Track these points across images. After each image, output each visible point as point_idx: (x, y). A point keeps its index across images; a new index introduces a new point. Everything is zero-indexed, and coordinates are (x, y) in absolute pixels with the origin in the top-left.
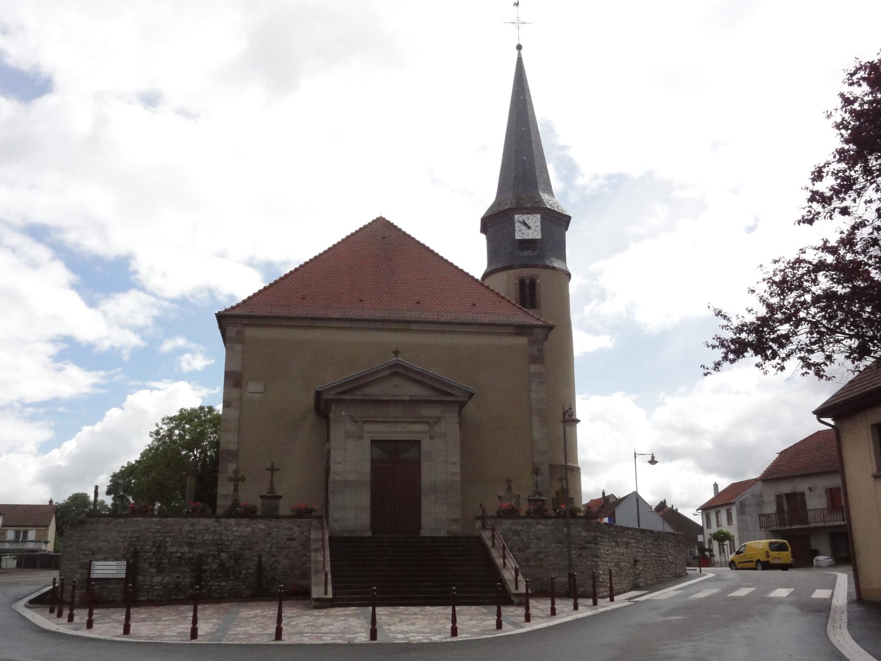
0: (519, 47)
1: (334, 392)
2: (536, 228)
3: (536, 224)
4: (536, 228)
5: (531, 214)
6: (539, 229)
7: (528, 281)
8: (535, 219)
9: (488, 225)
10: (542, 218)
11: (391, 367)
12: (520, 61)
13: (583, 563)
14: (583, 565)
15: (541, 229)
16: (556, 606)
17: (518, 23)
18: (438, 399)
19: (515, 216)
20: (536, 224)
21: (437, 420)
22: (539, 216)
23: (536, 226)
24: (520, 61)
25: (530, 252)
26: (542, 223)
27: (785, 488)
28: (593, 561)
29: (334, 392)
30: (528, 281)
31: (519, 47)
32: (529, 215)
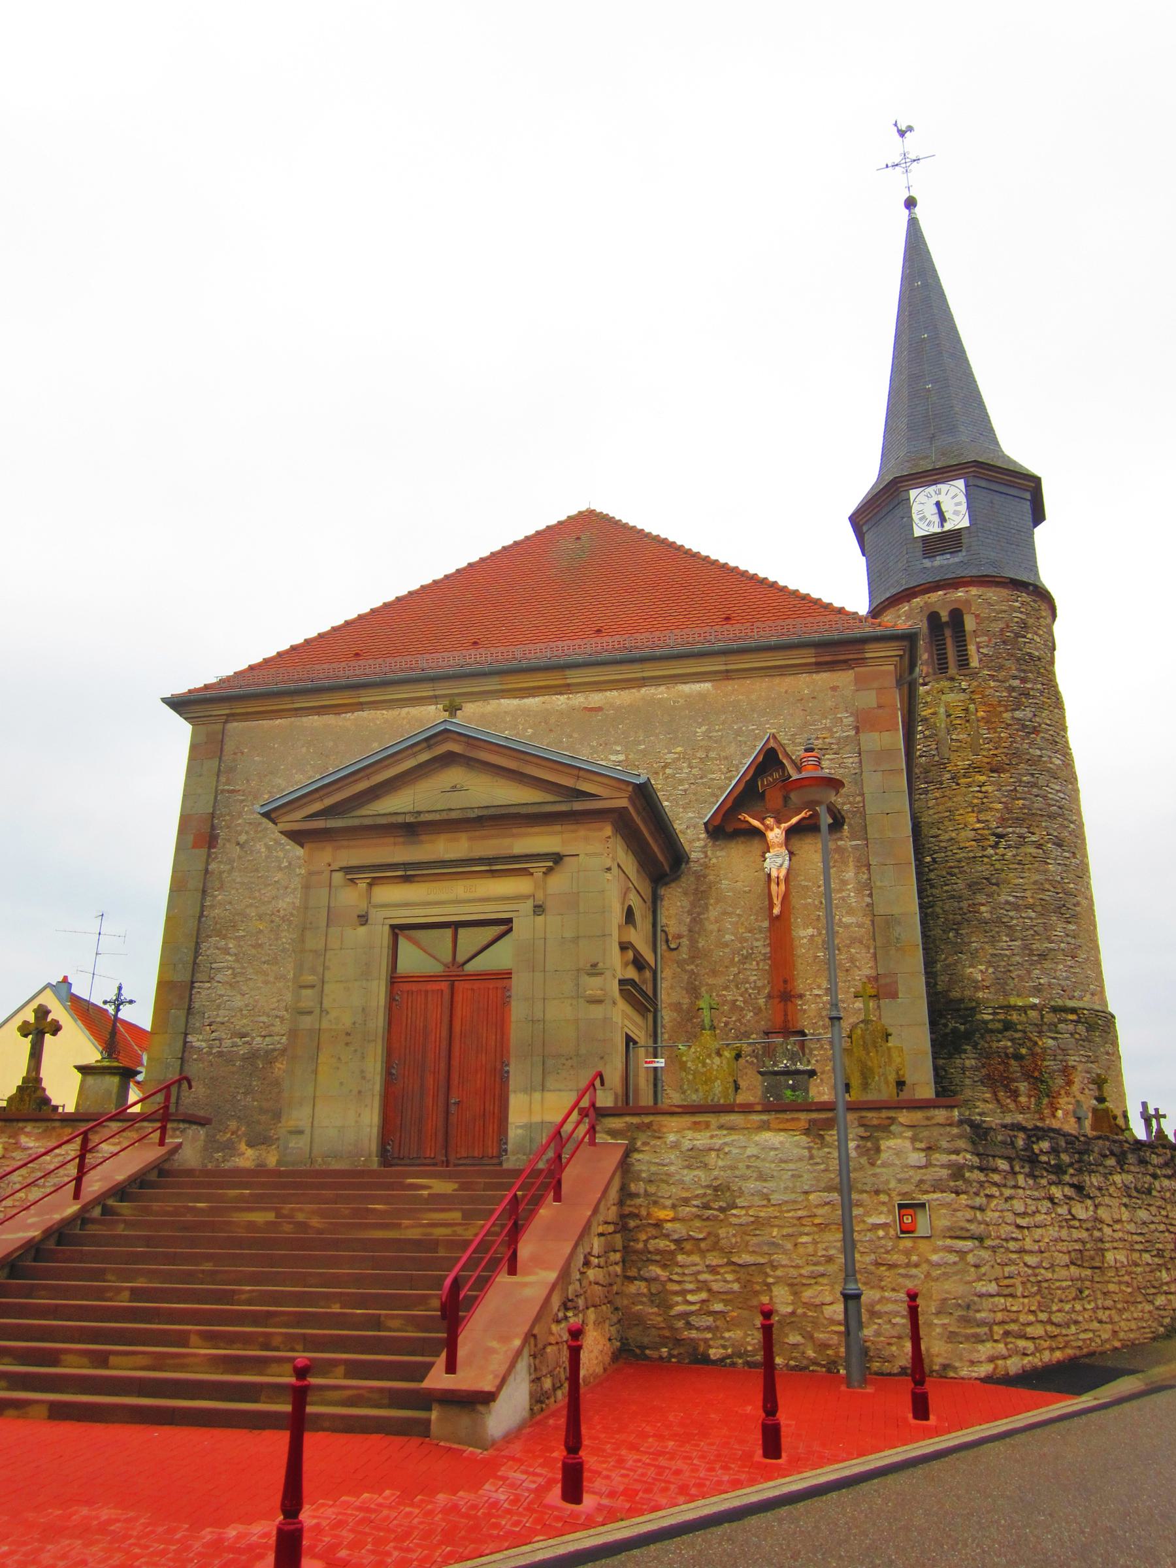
0: (910, 203)
1: (300, 814)
2: (958, 508)
3: (957, 500)
4: (958, 508)
5: (943, 483)
6: (963, 508)
7: (944, 616)
8: (953, 491)
9: (865, 529)
10: (967, 486)
11: (429, 741)
12: (913, 224)
13: (914, 1258)
14: (916, 1265)
15: (968, 508)
16: (784, 1418)
17: (906, 162)
18: (564, 808)
19: (911, 492)
20: (957, 500)
21: (551, 864)
22: (960, 483)
23: (958, 504)
24: (913, 224)
25: (948, 556)
26: (967, 495)
27: (308, 1131)
28: (950, 1250)
29: (300, 814)
30: (944, 616)
31: (910, 203)
32: (939, 486)
